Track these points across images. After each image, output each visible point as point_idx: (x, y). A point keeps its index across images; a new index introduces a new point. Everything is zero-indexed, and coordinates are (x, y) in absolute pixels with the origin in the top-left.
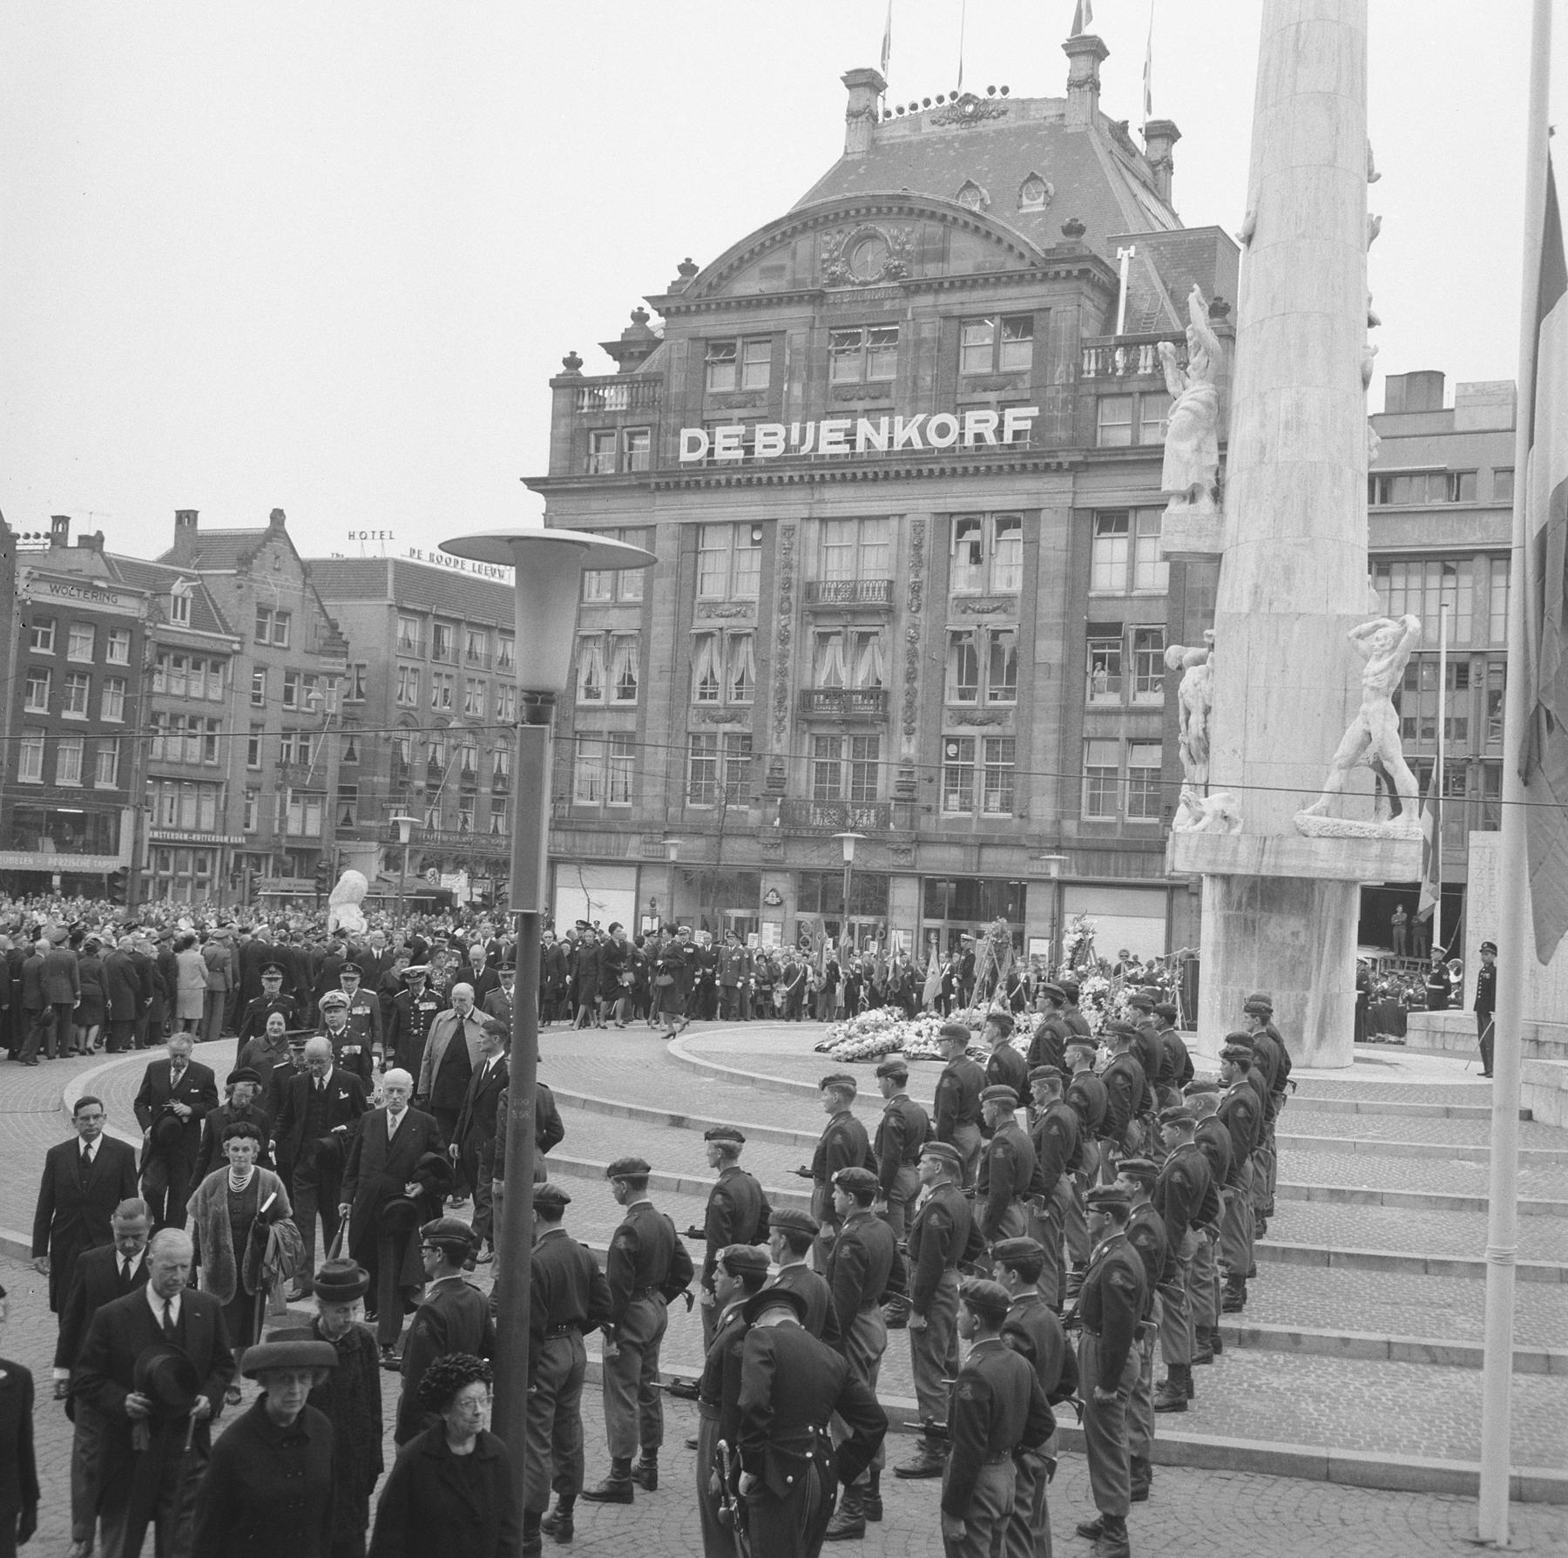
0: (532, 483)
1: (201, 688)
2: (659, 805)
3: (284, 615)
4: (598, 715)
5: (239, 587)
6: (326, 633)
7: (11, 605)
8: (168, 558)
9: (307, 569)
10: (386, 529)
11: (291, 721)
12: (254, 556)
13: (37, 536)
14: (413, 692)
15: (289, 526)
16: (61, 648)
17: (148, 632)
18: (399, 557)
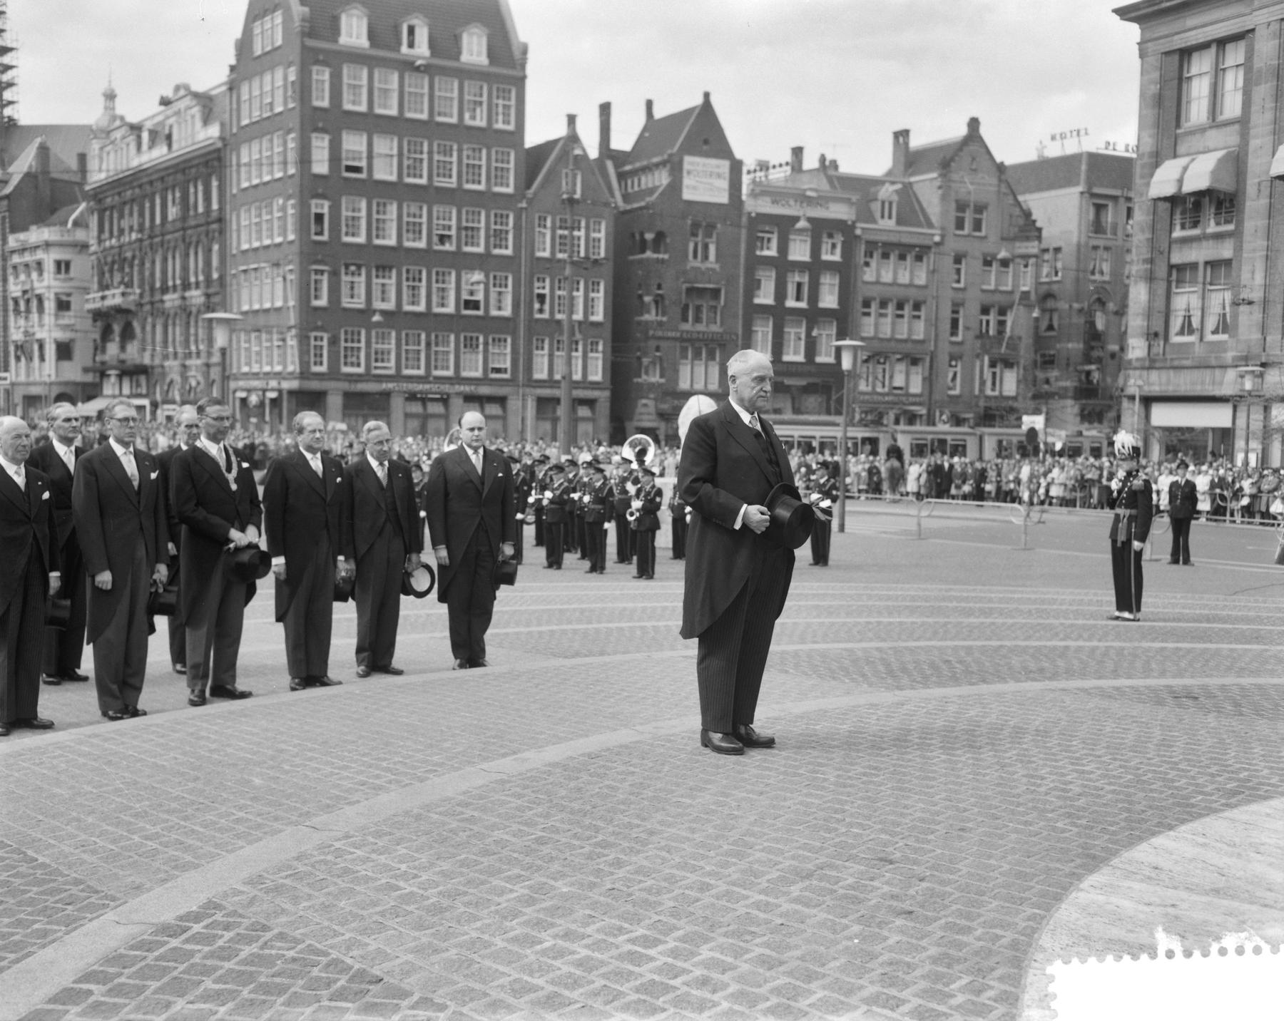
0: (1123, 13)
1: (907, 274)
2: (1256, 336)
3: (980, 209)
4: (1195, 245)
5: (940, 188)
6: (1021, 221)
7: (740, 216)
8: (889, 173)
9: (1001, 168)
10: (1082, 127)
11: (988, 299)
12: (952, 159)
13: (781, 165)
14: (1106, 267)
15: (984, 131)
16: (783, 248)
17: (858, 232)
18: (1093, 149)
